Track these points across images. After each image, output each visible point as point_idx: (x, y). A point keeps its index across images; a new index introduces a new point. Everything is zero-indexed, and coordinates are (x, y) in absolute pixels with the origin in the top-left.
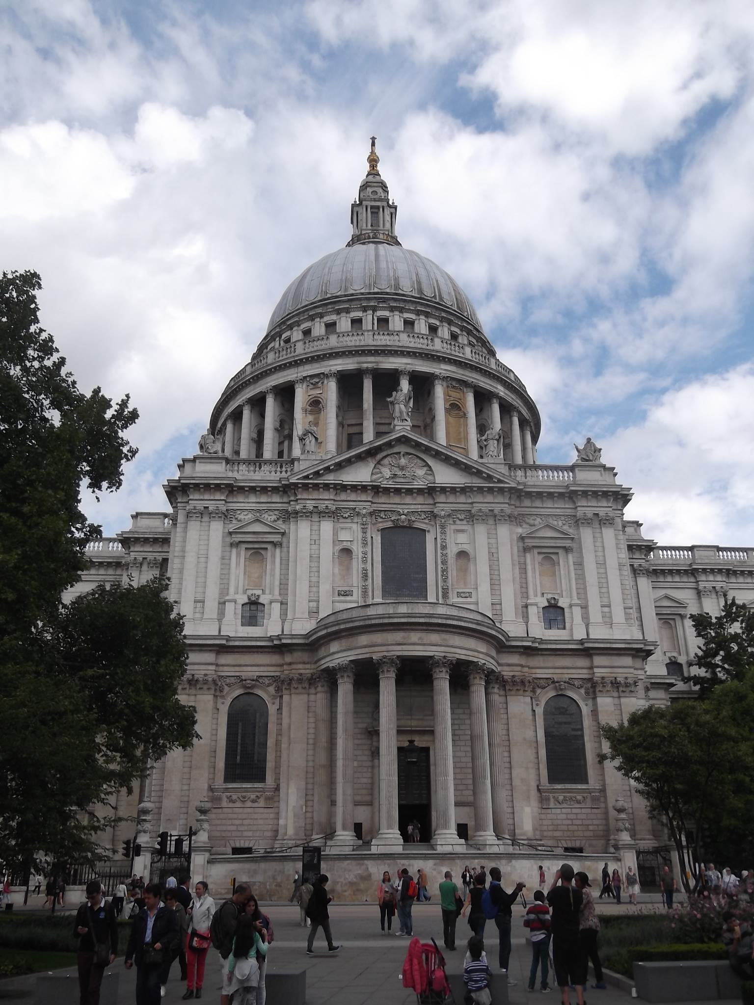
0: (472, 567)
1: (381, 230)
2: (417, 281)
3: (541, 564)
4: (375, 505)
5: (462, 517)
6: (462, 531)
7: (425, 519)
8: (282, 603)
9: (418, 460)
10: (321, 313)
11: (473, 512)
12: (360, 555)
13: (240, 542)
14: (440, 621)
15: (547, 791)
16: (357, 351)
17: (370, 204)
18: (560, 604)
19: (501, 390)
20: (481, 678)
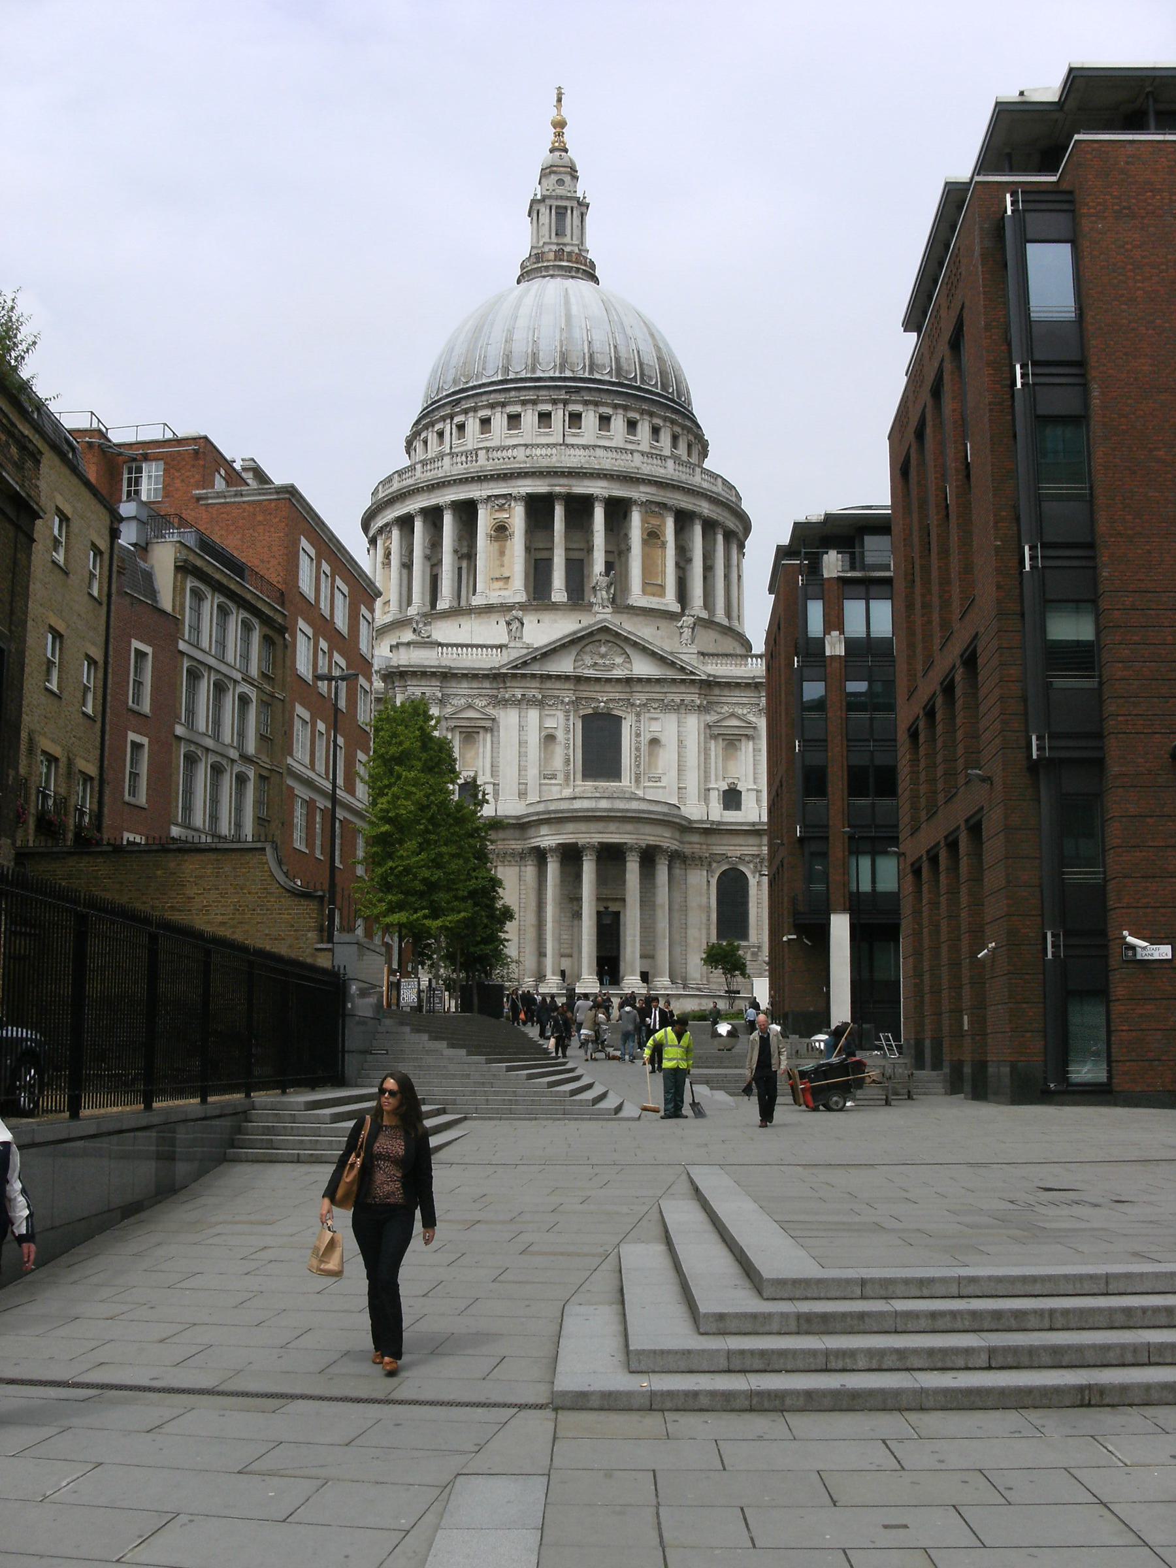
3: (725, 749)
6: (656, 719)
8: (494, 784)
9: (619, 649)
10: (503, 402)
12: (564, 742)
16: (549, 473)
17: (555, 203)
18: (738, 788)
19: (705, 508)
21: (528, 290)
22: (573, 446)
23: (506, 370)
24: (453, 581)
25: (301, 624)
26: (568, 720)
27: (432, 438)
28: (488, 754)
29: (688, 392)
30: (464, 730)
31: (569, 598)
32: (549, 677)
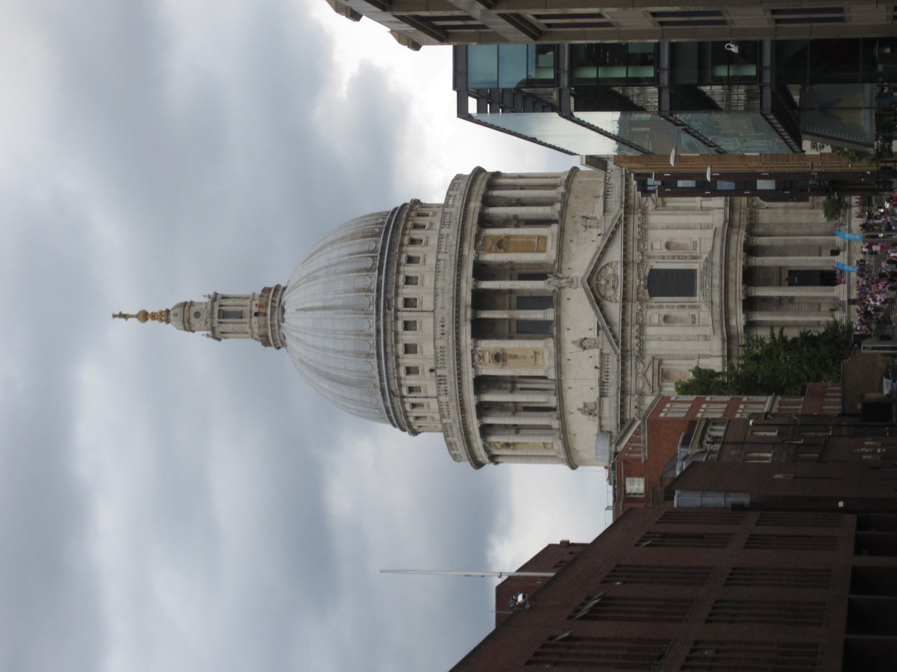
0: (677, 241)
1: (251, 308)
2: (357, 272)
4: (634, 300)
5: (642, 244)
6: (652, 245)
7: (643, 269)
8: (699, 358)
11: (640, 238)
12: (669, 310)
13: (658, 385)
14: (724, 261)
15: (813, 203)
17: (216, 320)
19: (475, 205)
20: (753, 239)
21: (298, 339)
22: (435, 304)
23: (368, 355)
24: (534, 394)
25: (699, 415)
26: (653, 307)
27: (416, 412)
28: (678, 362)
29: (371, 215)
30: (661, 379)
31: (553, 307)
32: (623, 320)
